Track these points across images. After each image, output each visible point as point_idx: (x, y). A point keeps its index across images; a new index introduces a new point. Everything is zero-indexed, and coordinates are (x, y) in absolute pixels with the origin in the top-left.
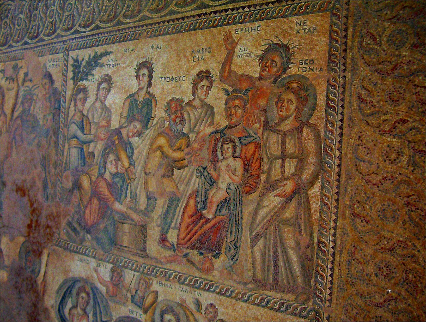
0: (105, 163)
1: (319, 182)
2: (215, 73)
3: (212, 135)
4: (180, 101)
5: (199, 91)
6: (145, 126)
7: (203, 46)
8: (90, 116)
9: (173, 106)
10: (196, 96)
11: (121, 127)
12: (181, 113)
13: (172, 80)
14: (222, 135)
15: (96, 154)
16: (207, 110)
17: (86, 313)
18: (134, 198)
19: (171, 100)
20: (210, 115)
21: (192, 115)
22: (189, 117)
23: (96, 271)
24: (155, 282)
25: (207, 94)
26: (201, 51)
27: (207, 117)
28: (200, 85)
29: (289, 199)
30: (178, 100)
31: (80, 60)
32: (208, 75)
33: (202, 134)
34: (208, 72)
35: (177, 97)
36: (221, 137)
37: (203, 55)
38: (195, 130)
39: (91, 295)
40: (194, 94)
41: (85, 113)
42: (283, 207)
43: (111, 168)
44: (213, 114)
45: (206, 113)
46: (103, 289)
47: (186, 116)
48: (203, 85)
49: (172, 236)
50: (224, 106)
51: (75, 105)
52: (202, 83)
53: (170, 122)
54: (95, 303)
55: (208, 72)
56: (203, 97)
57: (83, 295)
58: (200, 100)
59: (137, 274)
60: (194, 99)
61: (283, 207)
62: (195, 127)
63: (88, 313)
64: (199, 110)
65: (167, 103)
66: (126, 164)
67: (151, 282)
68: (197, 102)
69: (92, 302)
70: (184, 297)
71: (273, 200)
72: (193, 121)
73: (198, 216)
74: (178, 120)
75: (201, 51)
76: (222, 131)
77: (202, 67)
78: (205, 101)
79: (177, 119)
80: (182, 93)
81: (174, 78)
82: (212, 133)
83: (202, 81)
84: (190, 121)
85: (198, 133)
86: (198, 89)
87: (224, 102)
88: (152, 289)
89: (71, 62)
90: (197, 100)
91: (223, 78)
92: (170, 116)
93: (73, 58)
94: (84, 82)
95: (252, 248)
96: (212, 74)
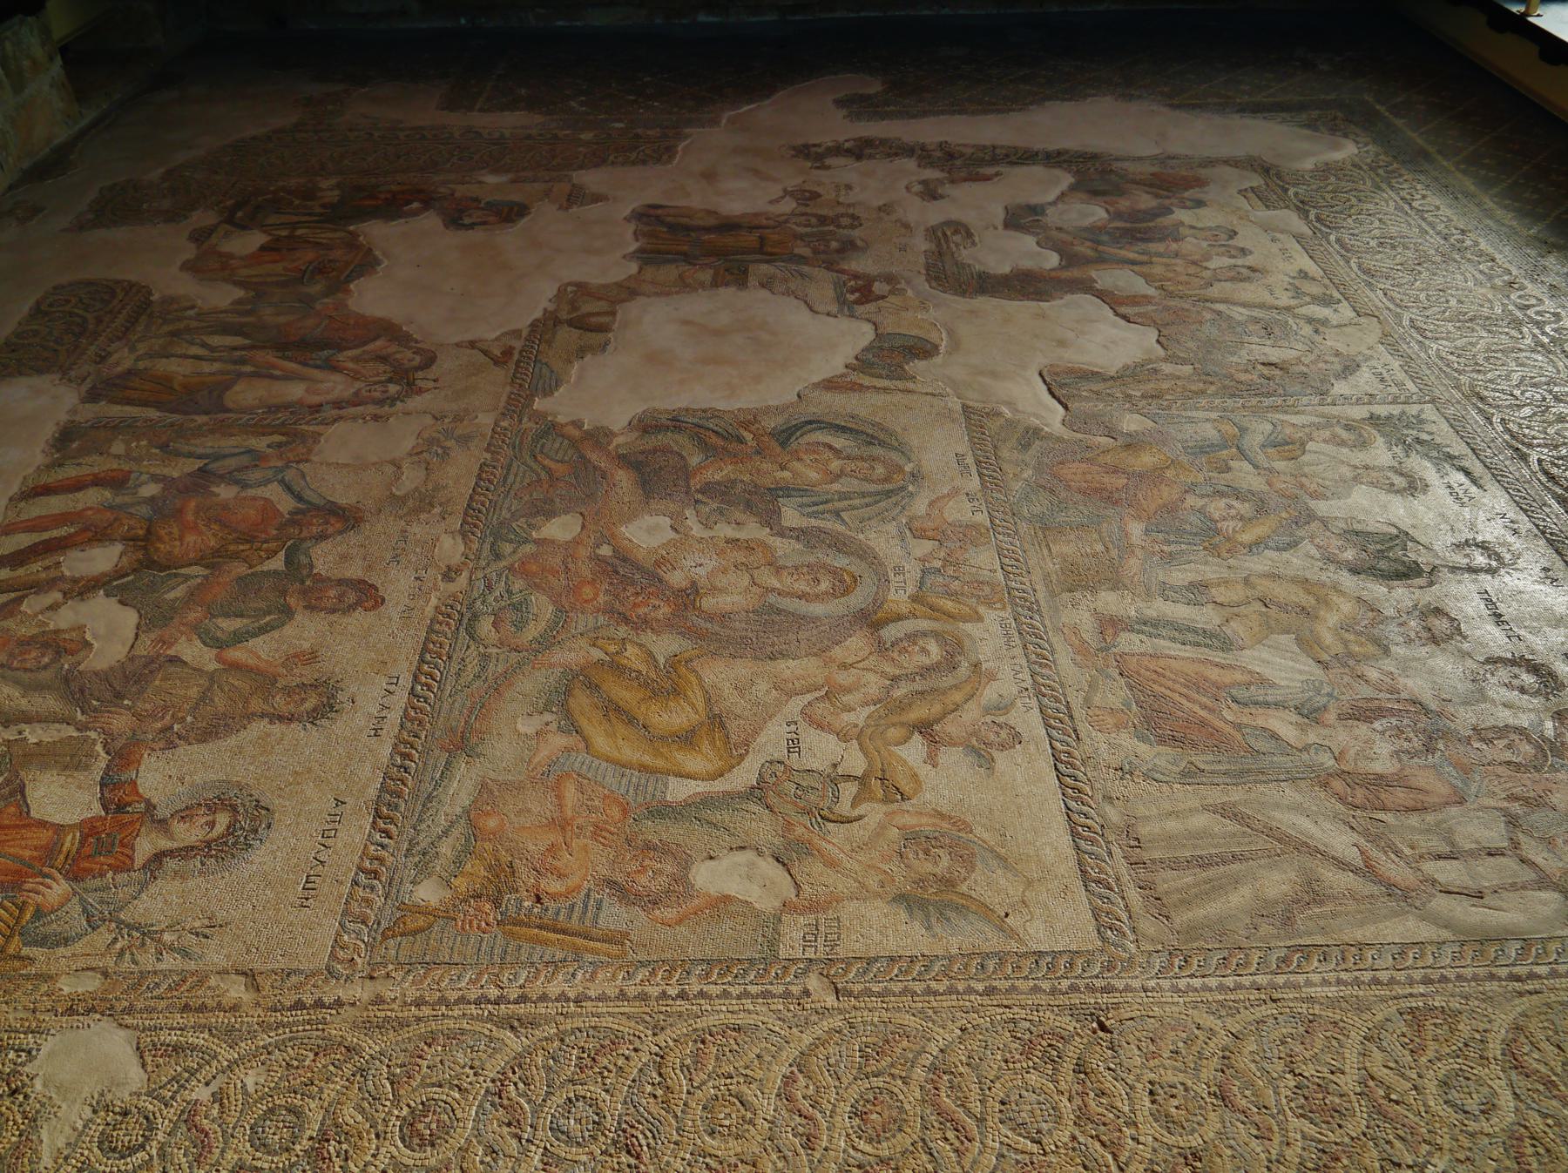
0: (1222, 495)
1: (1446, 934)
6: (1355, 571)
8: (1306, 458)
11: (1324, 522)
15: (1227, 476)
17: (839, 476)
18: (1169, 559)
23: (955, 492)
24: (1002, 614)
29: (1368, 870)
31: (1428, 427)
39: (888, 487)
41: (1310, 446)
42: (1341, 864)
43: (1217, 507)
46: (920, 506)
49: (1130, 642)
51: (1318, 427)
54: (870, 494)
57: (880, 470)
59: (1000, 575)
61: (1341, 864)
63: (842, 481)
66: (1246, 537)
67: (998, 605)
69: (872, 488)
70: (1000, 676)
71: (1343, 842)
73: (1218, 691)
88: (982, 609)
89: (1413, 410)
93: (1422, 410)
94: (1380, 440)
95: (1206, 808)
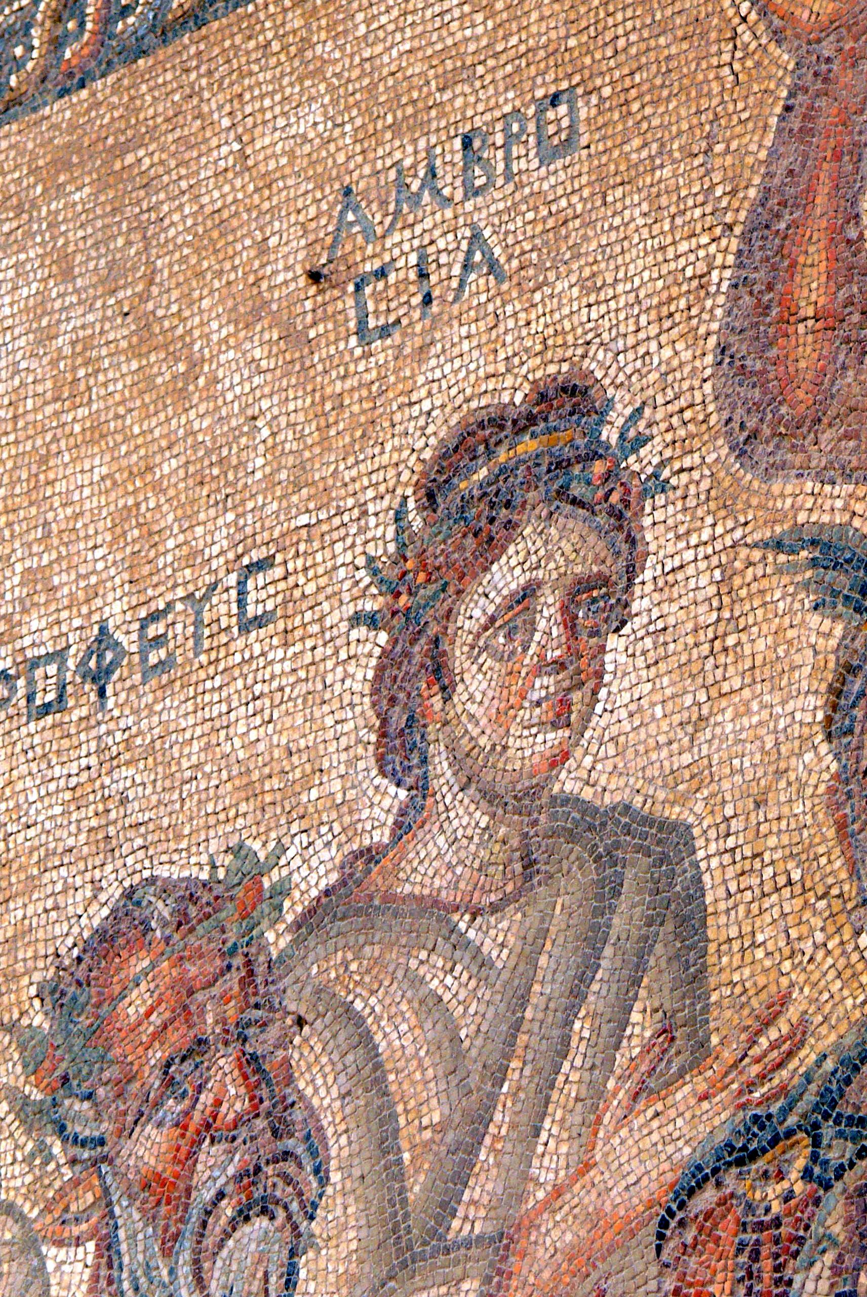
2: (659, 374)
3: (708, 1197)
4: (220, 910)
5: (477, 685)
7: (470, 105)
9: (135, 1004)
10: (441, 767)
12: (252, 1066)
13: (99, 679)
14: (837, 1151)
16: (608, 892)
19: (105, 944)
20: (645, 945)
21: (398, 1036)
22: (371, 1074)
25: (580, 671)
26: (450, 183)
27: (599, 993)
28: (474, 612)
30: (194, 903)
32: (569, 437)
33: (557, 1235)
34: (569, 398)
35: (189, 867)
36: (820, 1178)
37: (483, 212)
38: (470, 1221)
40: (399, 746)
44: (683, 916)
45: (593, 939)
47: (320, 1084)
48: (527, 595)
50: (820, 763)
52: (505, 576)
53: (108, 1249)
55: (569, 398)
56: (530, 745)
58: (489, 796)
60: (402, 828)
62: (461, 1178)
64: (497, 938)
65: (53, 995)
68: (453, 848)
72: (426, 1108)
74: (215, 1168)
75: (450, 183)
76: (828, 1103)
77: (469, 369)
78: (567, 783)
79: (210, 1155)
80: (250, 791)
81: (128, 641)
82: (698, 1178)
83: (490, 547)
84: (386, 1142)
85: (504, 1244)
86: (459, 658)
87: (811, 708)
90: (464, 815)
91: (766, 418)
92: (94, 1154)
96: (618, 416)
